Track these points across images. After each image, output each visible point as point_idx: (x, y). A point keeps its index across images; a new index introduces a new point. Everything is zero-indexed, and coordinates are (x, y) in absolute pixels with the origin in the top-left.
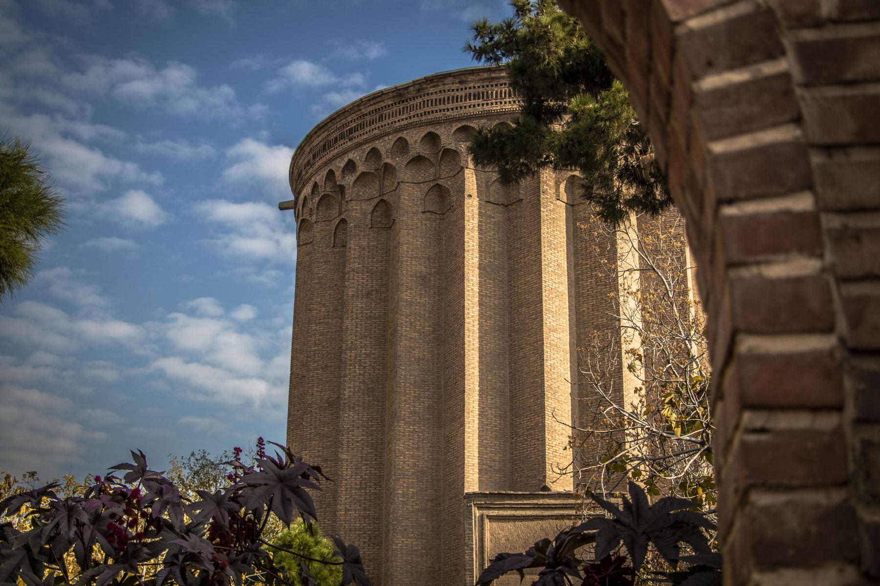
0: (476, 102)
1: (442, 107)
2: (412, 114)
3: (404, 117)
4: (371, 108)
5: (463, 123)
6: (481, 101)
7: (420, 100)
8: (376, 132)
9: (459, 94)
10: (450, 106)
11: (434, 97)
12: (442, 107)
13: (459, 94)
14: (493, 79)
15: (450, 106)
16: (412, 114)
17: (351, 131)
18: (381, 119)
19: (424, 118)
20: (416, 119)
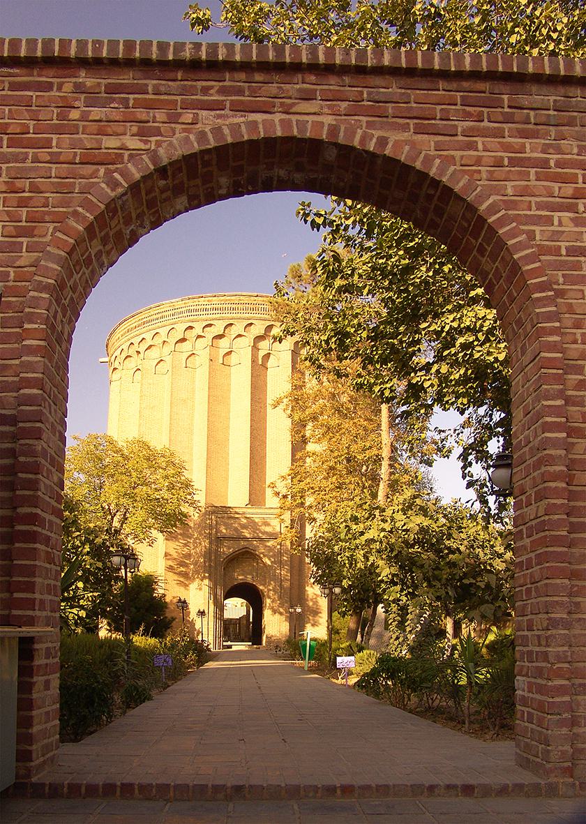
0: (217, 312)
1: (197, 313)
2: (180, 316)
3: (175, 317)
4: (157, 312)
5: (209, 322)
6: (219, 312)
7: (184, 309)
8: (160, 324)
9: (207, 307)
10: (202, 313)
11: (192, 308)
12: (197, 313)
13: (207, 307)
14: (227, 300)
15: (202, 313)
16: (180, 316)
17: (144, 323)
18: (162, 317)
19: (187, 318)
20: (182, 319)
